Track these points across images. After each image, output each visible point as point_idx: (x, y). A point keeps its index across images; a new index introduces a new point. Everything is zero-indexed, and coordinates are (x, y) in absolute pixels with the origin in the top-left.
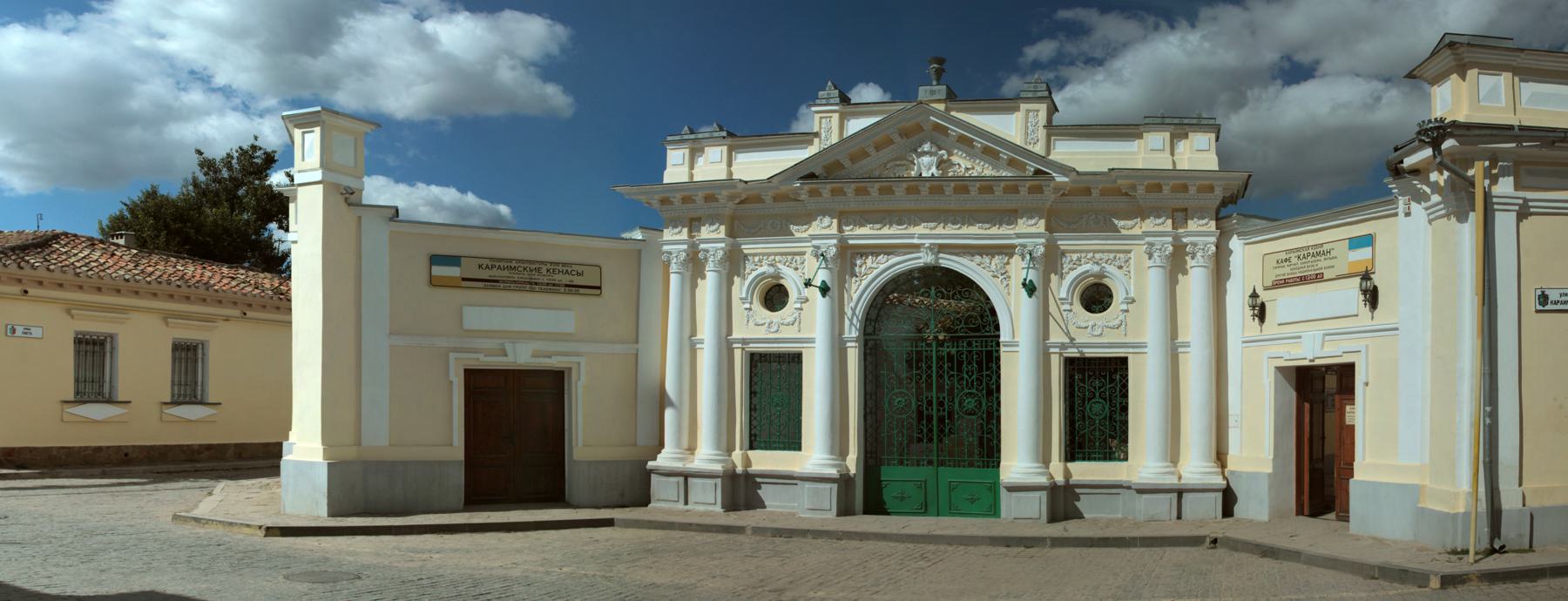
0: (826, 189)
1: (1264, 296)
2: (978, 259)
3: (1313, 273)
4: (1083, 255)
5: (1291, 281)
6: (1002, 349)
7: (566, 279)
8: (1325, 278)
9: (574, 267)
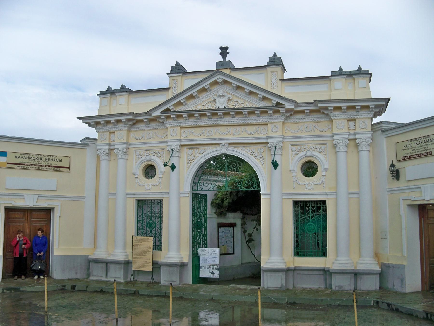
1: (398, 166)
3: (425, 152)
4: (303, 147)
5: (413, 157)
7: (54, 163)
9: (58, 158)
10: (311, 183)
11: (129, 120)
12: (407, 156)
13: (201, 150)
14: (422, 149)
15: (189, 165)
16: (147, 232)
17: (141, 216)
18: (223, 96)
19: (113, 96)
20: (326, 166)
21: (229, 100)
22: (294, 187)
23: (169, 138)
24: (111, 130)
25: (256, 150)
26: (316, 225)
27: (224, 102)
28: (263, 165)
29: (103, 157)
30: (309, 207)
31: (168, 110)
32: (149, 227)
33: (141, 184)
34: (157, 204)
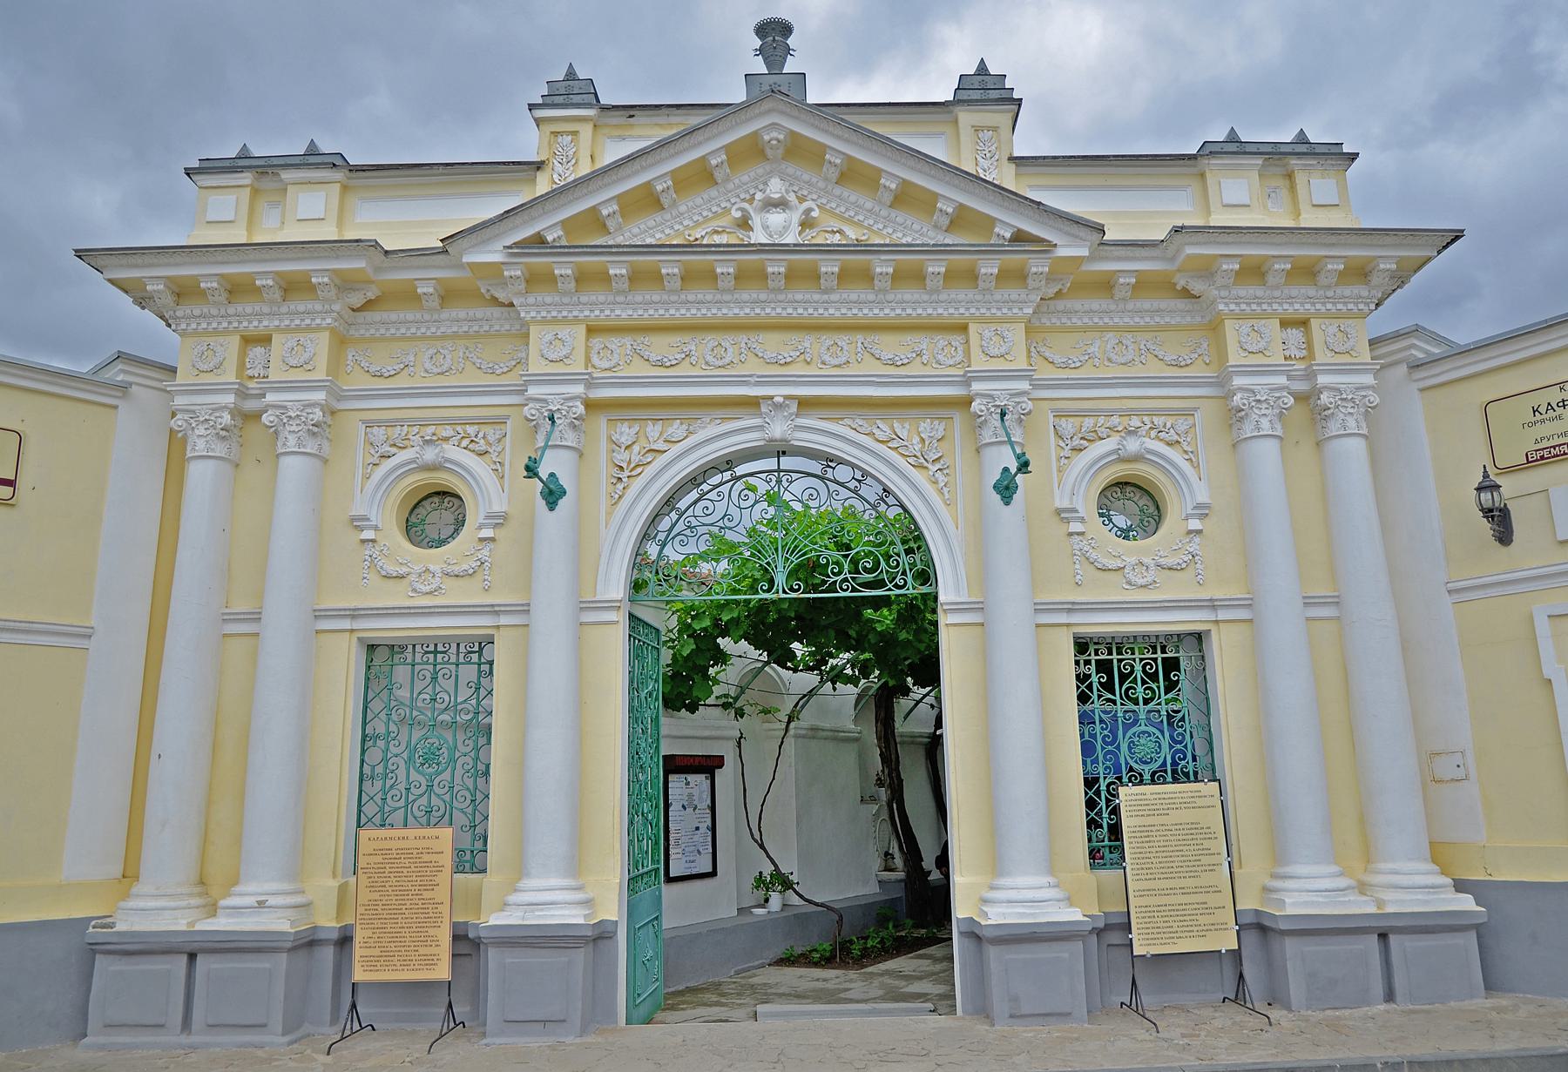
0: (564, 268)
1: (1509, 486)
2: (883, 430)
4: (1101, 420)
6: (944, 619)
10: (1146, 560)
11: (346, 283)
12: (1554, 447)
13: (677, 430)
15: (620, 486)
16: (408, 789)
17: (383, 716)
18: (781, 204)
19: (267, 183)
20: (1202, 497)
21: (807, 223)
22: (1079, 577)
23: (536, 366)
24: (254, 327)
25: (917, 431)
26: (1167, 735)
27: (786, 228)
28: (946, 490)
29: (199, 443)
30: (1134, 660)
31: (539, 241)
32: (423, 764)
33: (392, 569)
34: (461, 660)
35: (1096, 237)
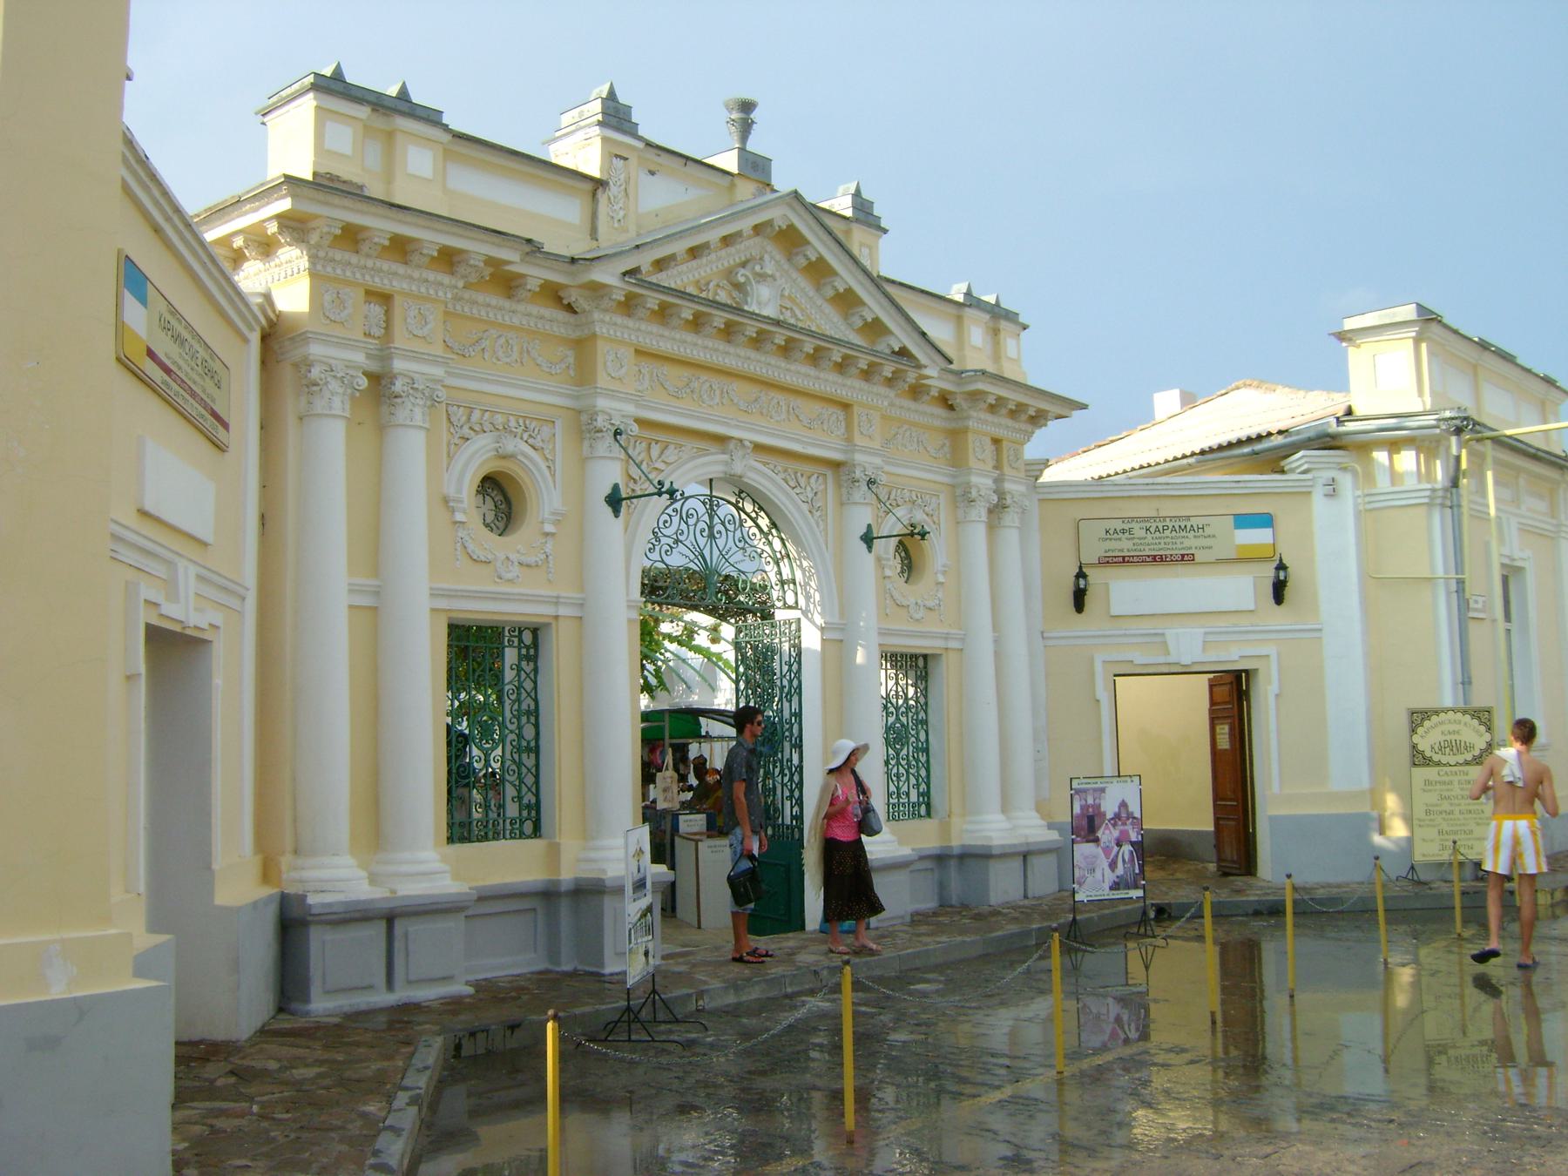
5: (1135, 559)
8: (1197, 559)
10: (919, 602)
14: (1165, 544)
35: (944, 364)
